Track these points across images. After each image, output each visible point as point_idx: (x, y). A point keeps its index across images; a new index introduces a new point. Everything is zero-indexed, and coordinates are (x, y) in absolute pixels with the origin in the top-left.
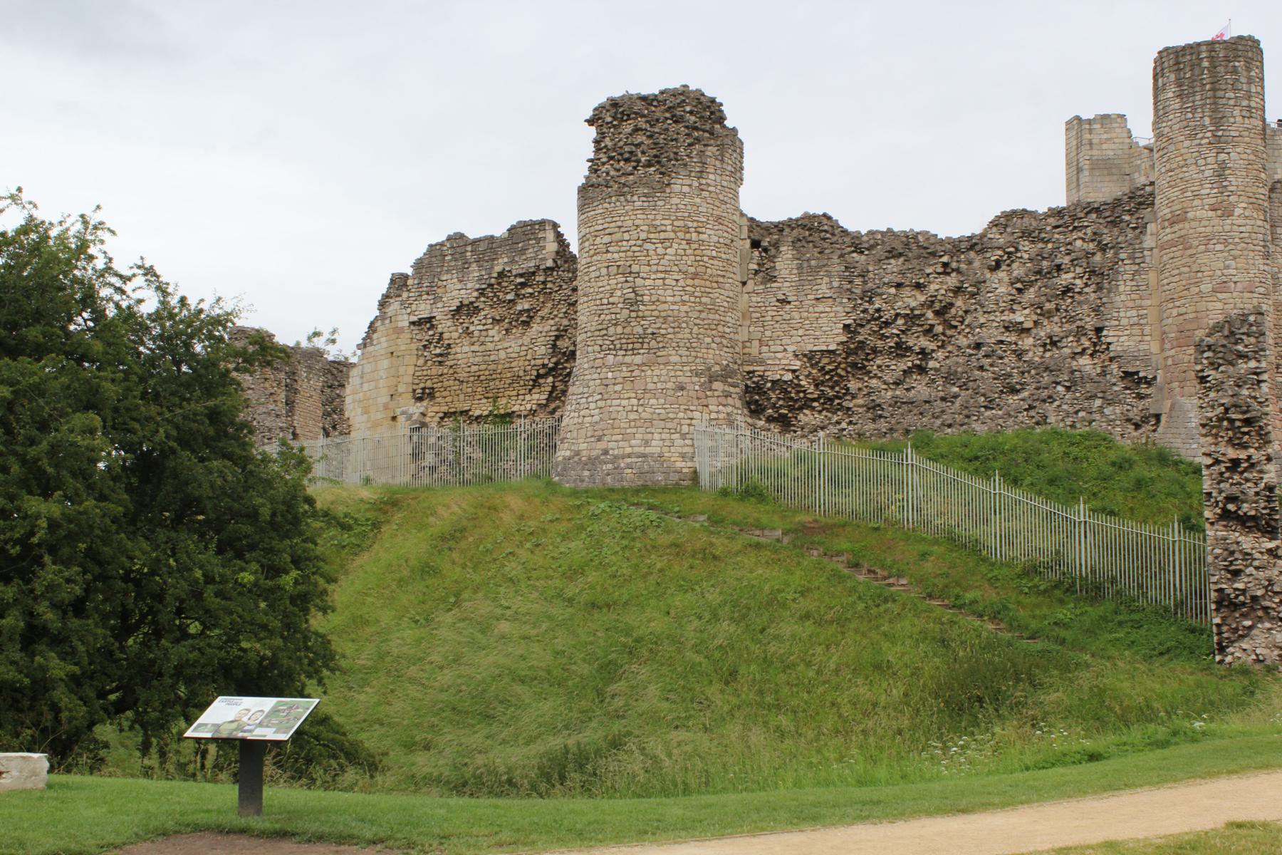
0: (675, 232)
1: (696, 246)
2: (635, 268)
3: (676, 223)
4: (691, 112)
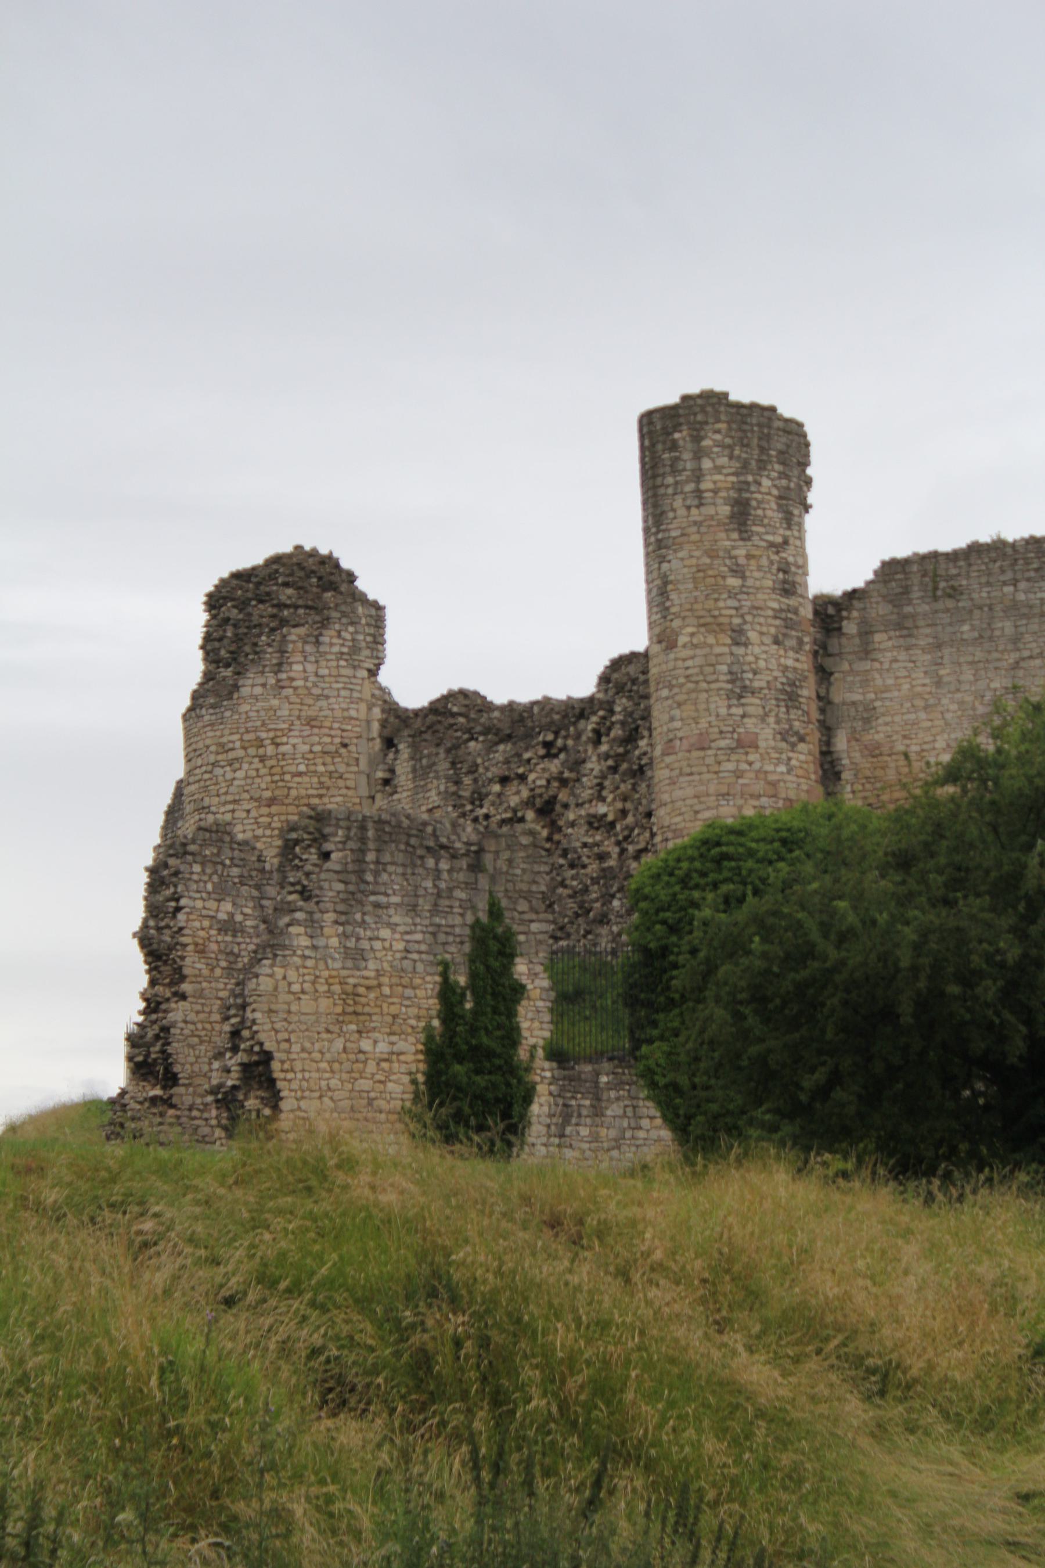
0: (245, 748)
1: (273, 762)
2: (207, 802)
3: (246, 737)
4: (286, 585)
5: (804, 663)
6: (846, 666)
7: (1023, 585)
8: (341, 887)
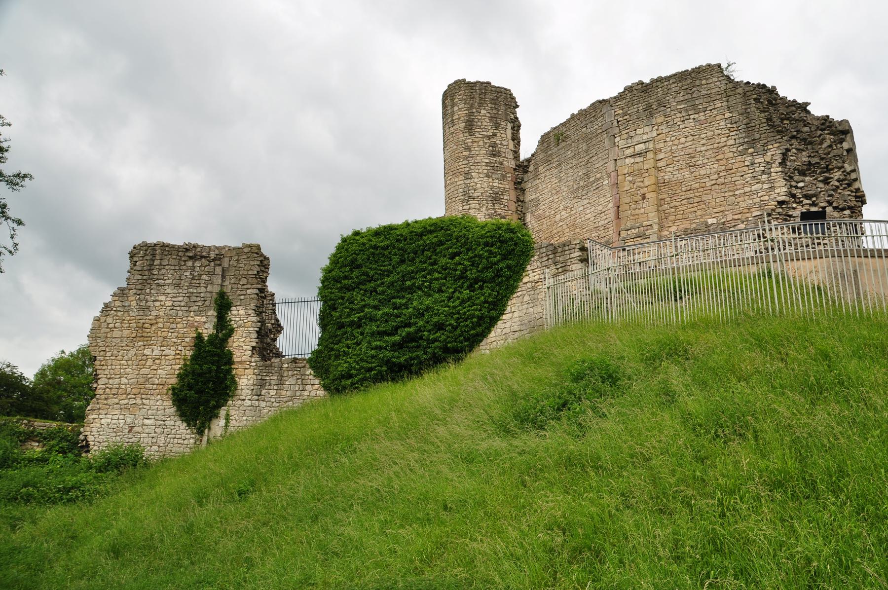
5: (508, 185)
6: (530, 185)
7: (588, 126)
8: (140, 277)
